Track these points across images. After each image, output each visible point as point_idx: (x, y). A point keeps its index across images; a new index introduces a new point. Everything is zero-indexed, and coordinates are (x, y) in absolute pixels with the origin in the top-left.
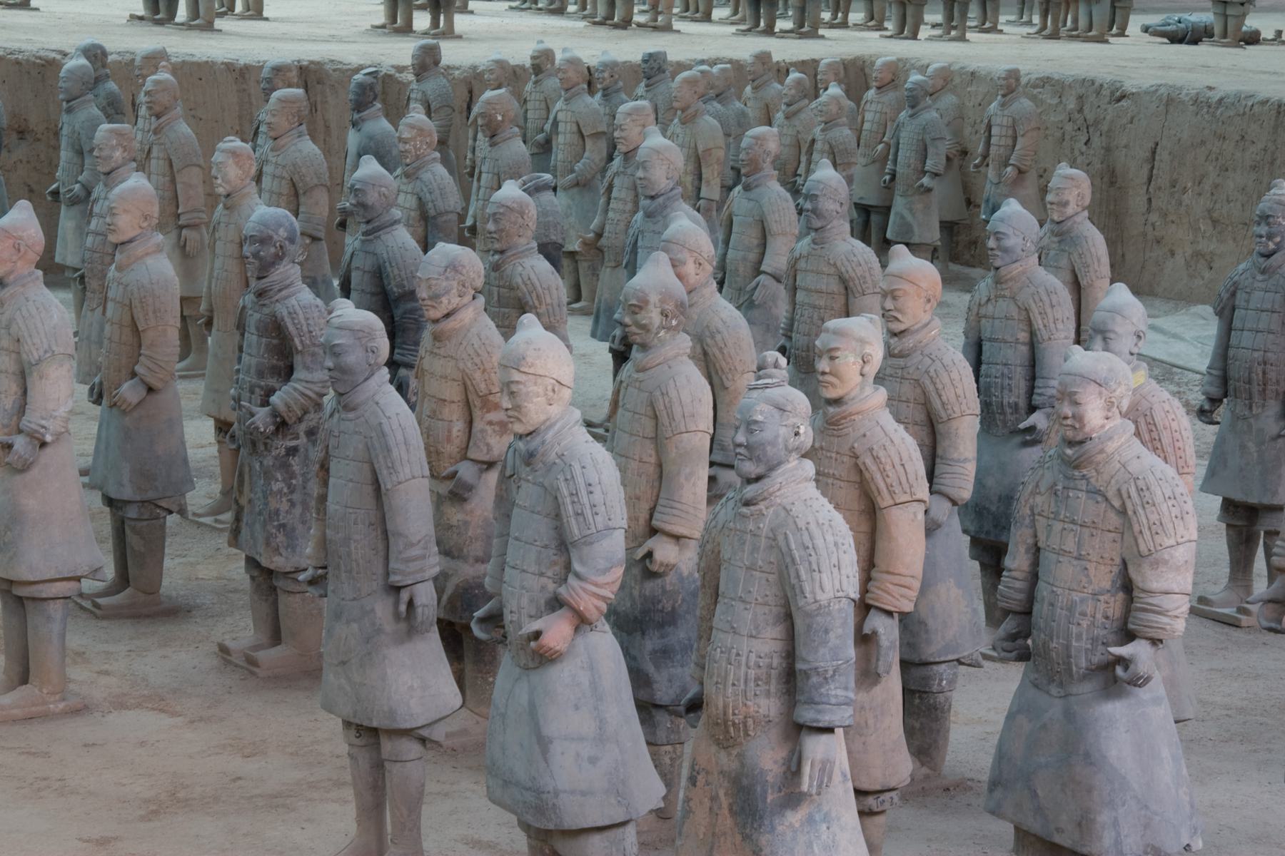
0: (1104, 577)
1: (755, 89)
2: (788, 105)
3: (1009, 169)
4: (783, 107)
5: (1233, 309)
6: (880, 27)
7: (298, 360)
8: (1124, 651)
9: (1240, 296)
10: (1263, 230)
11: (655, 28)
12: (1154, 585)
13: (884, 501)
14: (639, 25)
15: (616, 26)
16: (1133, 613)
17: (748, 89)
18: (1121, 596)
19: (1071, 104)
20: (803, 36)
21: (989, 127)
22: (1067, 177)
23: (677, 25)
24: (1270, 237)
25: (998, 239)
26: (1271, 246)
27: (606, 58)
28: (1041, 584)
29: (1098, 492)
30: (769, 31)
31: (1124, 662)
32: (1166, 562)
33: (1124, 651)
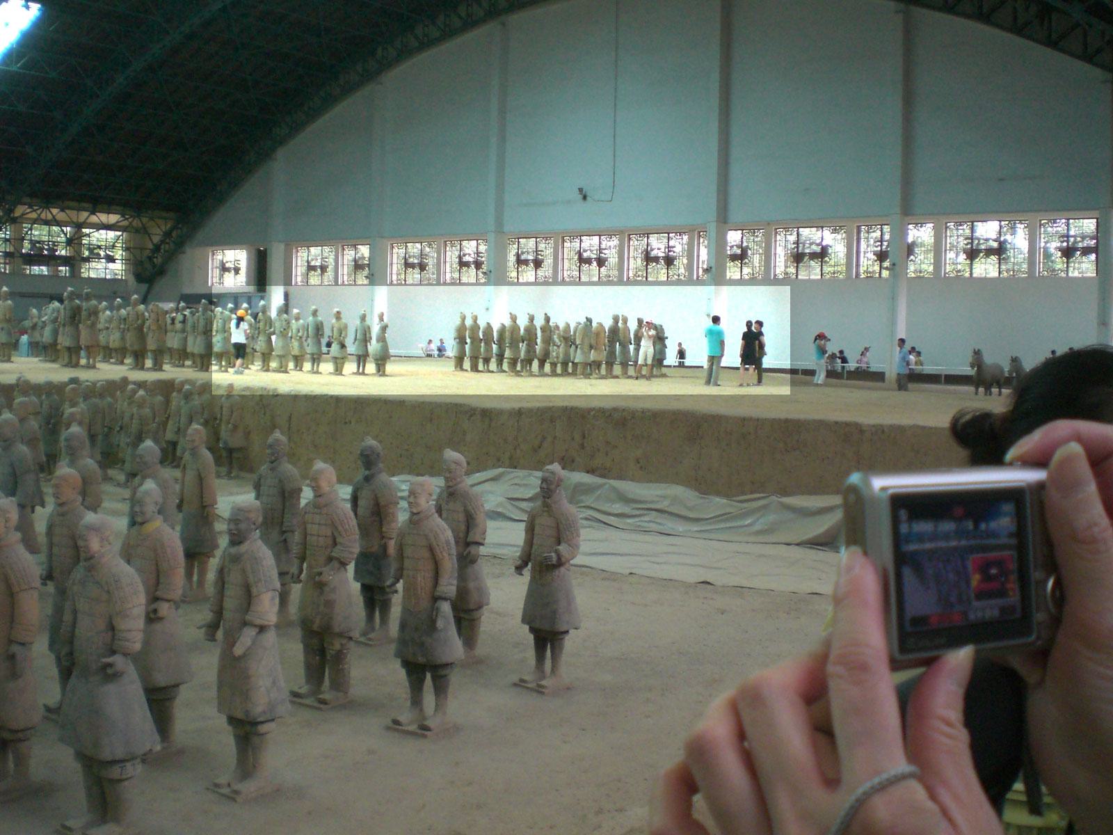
0: (102, 625)
1: (121, 392)
2: (129, 399)
3: (230, 425)
4: (127, 400)
5: (260, 486)
6: (196, 367)
8: (109, 660)
9: (262, 480)
12: (123, 627)
13: (16, 589)
14: (82, 366)
15: (72, 367)
16: (116, 642)
17: (118, 392)
18: (110, 633)
20: (155, 370)
21: (222, 408)
22: (196, 430)
23: (98, 365)
24: (273, 454)
25: (141, 458)
26: (273, 458)
27: (47, 380)
28: (77, 630)
29: (97, 583)
30: (142, 368)
31: (110, 665)
32: (128, 616)
33: (109, 660)
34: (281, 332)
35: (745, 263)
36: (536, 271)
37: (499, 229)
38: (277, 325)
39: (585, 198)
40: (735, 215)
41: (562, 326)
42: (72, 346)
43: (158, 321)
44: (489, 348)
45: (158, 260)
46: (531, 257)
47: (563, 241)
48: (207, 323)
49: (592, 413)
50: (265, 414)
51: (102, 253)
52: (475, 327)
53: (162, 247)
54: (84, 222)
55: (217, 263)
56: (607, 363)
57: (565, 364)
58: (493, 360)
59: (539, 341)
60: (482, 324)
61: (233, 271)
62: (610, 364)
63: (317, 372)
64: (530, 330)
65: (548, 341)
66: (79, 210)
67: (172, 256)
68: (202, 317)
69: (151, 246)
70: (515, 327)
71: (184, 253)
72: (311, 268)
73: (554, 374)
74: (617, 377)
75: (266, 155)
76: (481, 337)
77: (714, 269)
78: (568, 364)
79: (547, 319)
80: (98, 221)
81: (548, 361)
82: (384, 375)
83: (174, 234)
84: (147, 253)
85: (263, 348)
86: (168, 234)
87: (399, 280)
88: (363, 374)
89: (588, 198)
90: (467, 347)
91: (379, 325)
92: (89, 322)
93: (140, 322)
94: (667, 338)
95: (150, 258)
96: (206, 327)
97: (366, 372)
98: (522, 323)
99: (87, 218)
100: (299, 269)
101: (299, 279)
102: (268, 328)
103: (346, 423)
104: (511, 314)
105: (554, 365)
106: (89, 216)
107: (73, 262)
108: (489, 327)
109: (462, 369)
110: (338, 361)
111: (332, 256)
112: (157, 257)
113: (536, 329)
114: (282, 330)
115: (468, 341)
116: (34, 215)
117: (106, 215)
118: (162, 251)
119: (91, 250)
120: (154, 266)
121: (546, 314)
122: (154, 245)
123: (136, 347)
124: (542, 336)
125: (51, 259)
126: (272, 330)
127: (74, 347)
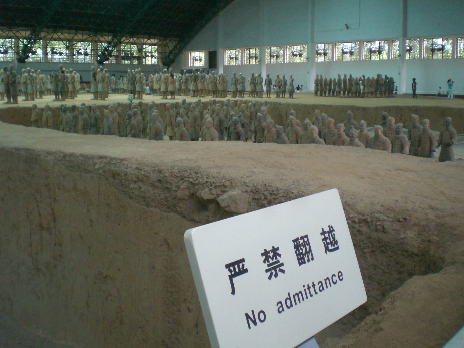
7: (241, 137)
10: (348, 117)
11: (202, 97)
15: (196, 97)
19: (273, 106)
24: (349, 117)
34: (260, 83)
35: (412, 53)
36: (325, 57)
37: (312, 42)
38: (259, 80)
39: (348, 28)
40: (409, 35)
41: (355, 78)
42: (195, 89)
43: (223, 80)
44: (326, 88)
45: (171, 57)
46: (322, 52)
47: (336, 45)
48: (236, 80)
49: (405, 108)
50: (276, 111)
51: (150, 55)
52: (321, 79)
53: (173, 51)
54: (146, 43)
55: (192, 57)
56: (375, 92)
57: (356, 93)
58: (327, 92)
59: (348, 84)
60: (324, 78)
61: (199, 60)
62: (376, 92)
63: (269, 97)
64: (339, 80)
65: (351, 84)
66: (144, 38)
67: (177, 55)
68: (234, 78)
69: (169, 51)
70: (339, 80)
71: (182, 54)
72: (231, 58)
73: (352, 97)
74: (378, 97)
75: (215, 14)
76: (323, 84)
77: (401, 55)
78: (357, 93)
79: (351, 76)
80: (151, 42)
81: (351, 92)
82: (292, 98)
83: (178, 46)
84: (167, 54)
85: (253, 89)
86: (175, 47)
87: (268, 62)
88: (284, 98)
89: (349, 28)
90: (319, 87)
91: (291, 80)
92: (203, 81)
93: (216, 80)
94: (395, 82)
95: (168, 56)
96: (235, 82)
97: (285, 97)
98: (342, 77)
99: (147, 41)
100: (226, 59)
101: (226, 63)
102: (255, 81)
103: (309, 113)
104: (339, 74)
105: (352, 93)
106: (147, 40)
107: (139, 59)
108: (326, 79)
109: (318, 96)
110: (278, 93)
111: (240, 54)
112: (171, 56)
113: (347, 80)
114: (261, 82)
115: (319, 85)
116: (127, 41)
117: (154, 40)
118: (173, 53)
119: (145, 54)
120: (170, 59)
121: (350, 74)
122: (170, 51)
123: (214, 90)
124: (349, 83)
125: (131, 57)
126: (257, 82)
127: (196, 90)
